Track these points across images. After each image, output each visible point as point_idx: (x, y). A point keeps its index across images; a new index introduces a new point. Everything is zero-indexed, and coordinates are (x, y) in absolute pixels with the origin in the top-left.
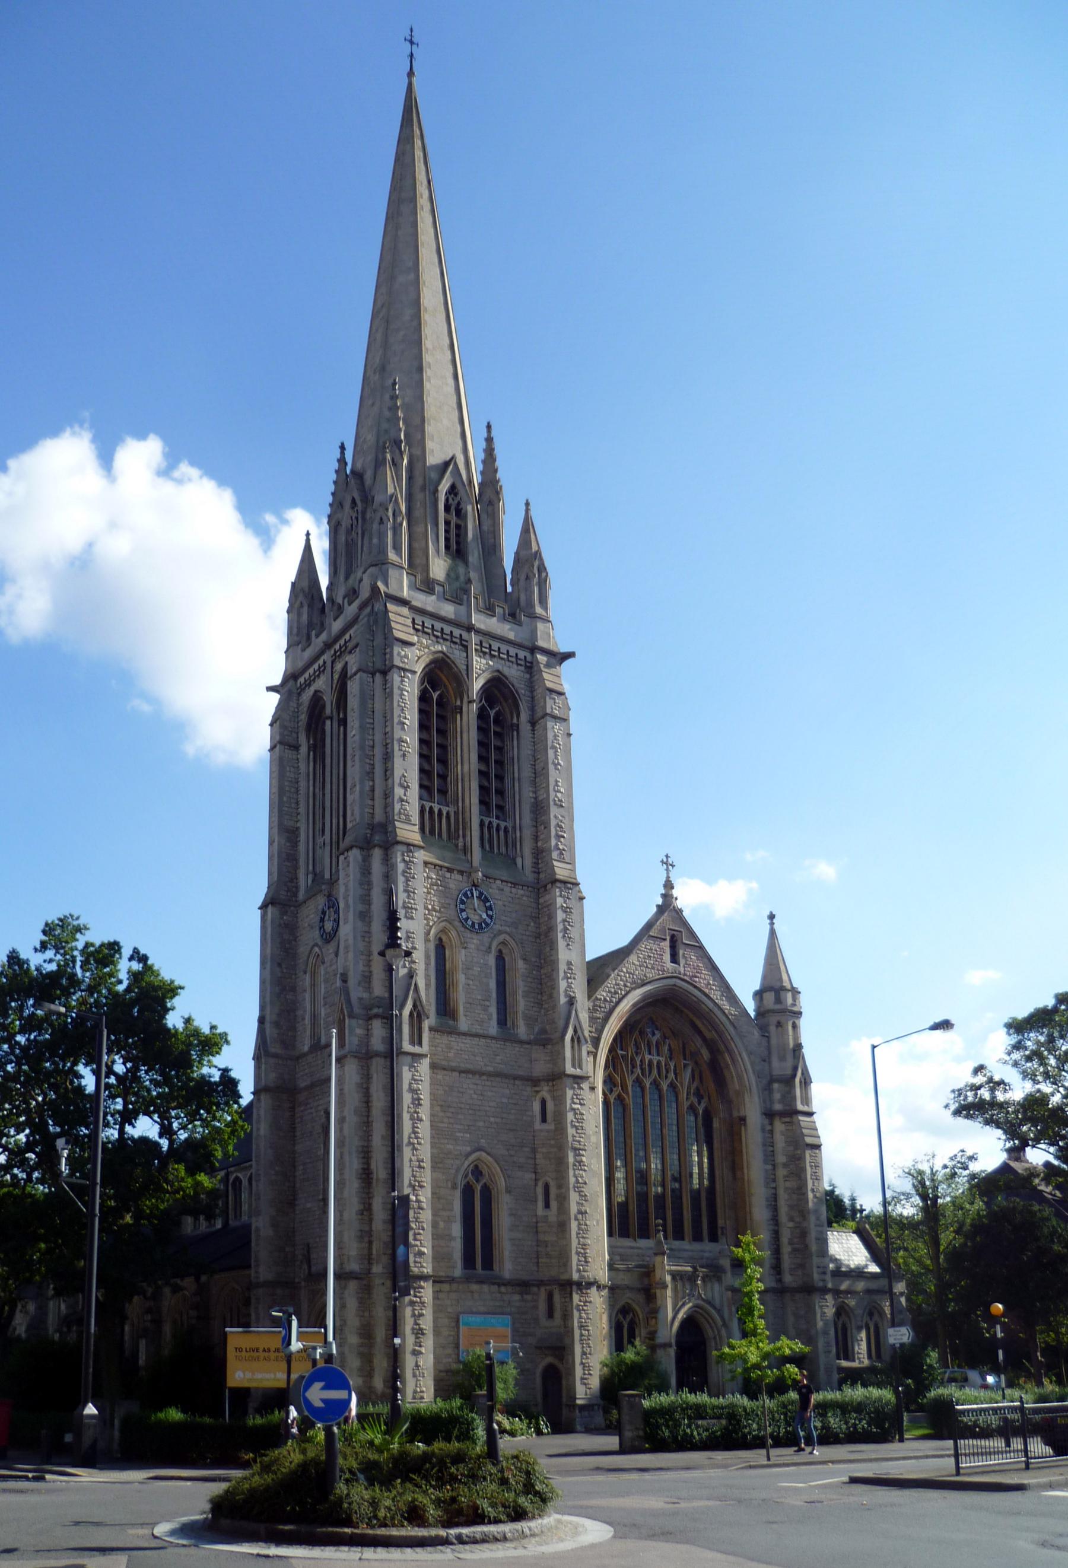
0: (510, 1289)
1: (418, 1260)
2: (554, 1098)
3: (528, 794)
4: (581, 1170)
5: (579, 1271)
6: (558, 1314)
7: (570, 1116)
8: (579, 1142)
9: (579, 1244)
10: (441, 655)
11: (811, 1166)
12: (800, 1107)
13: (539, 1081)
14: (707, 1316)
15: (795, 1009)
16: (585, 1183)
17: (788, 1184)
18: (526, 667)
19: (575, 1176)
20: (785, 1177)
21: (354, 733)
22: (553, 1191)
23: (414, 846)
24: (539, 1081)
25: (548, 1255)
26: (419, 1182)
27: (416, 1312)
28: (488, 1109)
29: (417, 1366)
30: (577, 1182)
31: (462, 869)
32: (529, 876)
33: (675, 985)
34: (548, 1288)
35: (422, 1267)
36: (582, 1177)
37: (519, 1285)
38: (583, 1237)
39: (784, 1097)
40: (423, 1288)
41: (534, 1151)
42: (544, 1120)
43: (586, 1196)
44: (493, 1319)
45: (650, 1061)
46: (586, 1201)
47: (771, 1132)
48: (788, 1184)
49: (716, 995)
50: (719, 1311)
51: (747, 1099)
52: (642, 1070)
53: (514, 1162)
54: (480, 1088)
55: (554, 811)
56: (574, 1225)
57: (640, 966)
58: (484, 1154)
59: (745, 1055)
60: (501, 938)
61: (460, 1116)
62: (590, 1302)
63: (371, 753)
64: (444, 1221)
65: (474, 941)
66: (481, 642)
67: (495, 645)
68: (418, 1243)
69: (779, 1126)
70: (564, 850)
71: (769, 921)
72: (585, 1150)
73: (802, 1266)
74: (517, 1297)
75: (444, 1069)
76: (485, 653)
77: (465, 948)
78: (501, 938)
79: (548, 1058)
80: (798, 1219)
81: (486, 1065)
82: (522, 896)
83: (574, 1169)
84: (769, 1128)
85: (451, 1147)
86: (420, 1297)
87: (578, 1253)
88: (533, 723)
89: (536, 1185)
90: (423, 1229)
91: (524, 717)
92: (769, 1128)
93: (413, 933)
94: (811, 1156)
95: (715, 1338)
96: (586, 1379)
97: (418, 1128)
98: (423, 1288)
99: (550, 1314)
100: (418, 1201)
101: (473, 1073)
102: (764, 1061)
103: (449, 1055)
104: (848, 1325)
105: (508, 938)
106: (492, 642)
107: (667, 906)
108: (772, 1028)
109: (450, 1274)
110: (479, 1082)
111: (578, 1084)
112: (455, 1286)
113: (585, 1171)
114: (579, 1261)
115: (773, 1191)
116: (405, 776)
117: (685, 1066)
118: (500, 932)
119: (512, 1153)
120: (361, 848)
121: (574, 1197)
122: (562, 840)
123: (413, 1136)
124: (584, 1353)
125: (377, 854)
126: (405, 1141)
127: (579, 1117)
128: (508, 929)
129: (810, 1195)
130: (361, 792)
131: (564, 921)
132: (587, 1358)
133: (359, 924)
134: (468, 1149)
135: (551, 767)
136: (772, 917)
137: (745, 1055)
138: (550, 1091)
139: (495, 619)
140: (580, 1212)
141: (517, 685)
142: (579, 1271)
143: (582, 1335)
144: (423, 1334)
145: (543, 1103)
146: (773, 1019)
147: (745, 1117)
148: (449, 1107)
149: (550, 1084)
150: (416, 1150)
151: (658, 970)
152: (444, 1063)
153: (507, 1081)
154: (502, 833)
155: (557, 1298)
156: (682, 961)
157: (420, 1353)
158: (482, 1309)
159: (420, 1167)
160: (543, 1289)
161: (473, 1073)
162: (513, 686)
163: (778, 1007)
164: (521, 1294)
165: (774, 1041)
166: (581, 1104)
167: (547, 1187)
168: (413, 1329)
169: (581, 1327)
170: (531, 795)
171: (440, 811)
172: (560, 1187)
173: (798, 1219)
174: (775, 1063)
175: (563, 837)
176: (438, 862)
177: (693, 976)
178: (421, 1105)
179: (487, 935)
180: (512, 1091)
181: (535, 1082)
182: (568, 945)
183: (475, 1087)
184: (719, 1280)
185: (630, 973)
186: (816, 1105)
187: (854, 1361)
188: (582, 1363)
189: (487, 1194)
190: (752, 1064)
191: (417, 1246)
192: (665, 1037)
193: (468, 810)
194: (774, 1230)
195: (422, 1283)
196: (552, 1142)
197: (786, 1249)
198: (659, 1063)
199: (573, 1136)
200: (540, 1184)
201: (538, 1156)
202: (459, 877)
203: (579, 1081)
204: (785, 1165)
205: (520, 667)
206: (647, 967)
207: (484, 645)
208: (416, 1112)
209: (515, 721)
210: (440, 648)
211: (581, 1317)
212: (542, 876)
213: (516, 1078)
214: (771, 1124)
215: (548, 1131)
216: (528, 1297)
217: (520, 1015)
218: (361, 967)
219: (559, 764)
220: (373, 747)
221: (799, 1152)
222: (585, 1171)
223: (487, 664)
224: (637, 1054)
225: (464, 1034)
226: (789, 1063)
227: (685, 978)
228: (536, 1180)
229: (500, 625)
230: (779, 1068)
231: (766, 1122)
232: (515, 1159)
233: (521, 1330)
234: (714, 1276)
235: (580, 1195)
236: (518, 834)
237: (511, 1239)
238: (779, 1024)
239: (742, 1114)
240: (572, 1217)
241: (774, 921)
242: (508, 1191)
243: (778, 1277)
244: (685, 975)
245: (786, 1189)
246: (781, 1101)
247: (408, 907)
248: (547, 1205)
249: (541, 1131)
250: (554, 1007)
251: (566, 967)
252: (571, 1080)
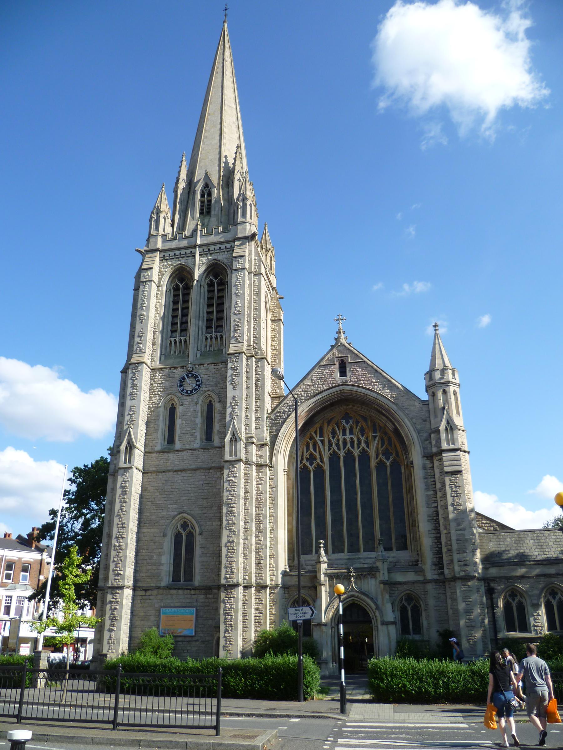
0: (197, 592)
1: (117, 578)
4: (232, 516)
5: (226, 578)
7: (226, 485)
8: (231, 499)
9: (227, 561)
10: (180, 265)
11: (451, 488)
12: (445, 446)
15: (443, 381)
16: (234, 524)
19: (227, 520)
23: (138, 363)
26: (121, 535)
27: (113, 607)
28: (190, 489)
29: (111, 638)
30: (228, 523)
31: (182, 365)
33: (343, 390)
35: (119, 582)
36: (232, 520)
37: (204, 589)
38: (230, 557)
40: (118, 593)
43: (234, 531)
44: (183, 610)
45: (344, 439)
46: (234, 534)
47: (433, 468)
49: (378, 388)
50: (372, 599)
51: (413, 449)
52: (338, 445)
53: (206, 517)
54: (186, 478)
55: (233, 318)
56: (224, 551)
57: (313, 385)
58: (185, 515)
59: (406, 420)
60: (207, 394)
61: (171, 496)
62: (234, 597)
64: (157, 555)
65: (189, 399)
66: (203, 250)
67: (212, 248)
68: (118, 569)
70: (239, 336)
72: (236, 504)
74: (202, 596)
75: (164, 472)
76: (206, 254)
77: (182, 405)
78: (207, 394)
81: (191, 465)
82: (221, 368)
83: (226, 516)
84: (431, 465)
85: (164, 513)
86: (116, 599)
87: (226, 567)
90: (121, 561)
92: (431, 465)
93: (134, 406)
94: (450, 480)
95: (373, 618)
96: (227, 647)
97: (123, 506)
98: (118, 593)
100: (120, 546)
101: (182, 471)
102: (425, 421)
103: (168, 464)
104: (525, 604)
105: (210, 393)
106: (209, 247)
107: (337, 344)
109: (158, 585)
110: (185, 475)
111: (233, 465)
112: (160, 592)
113: (235, 516)
114: (227, 572)
115: (434, 509)
116: (141, 331)
117: (375, 437)
118: (205, 392)
119: (204, 511)
121: (225, 533)
122: (238, 331)
123: (120, 511)
124: (226, 630)
126: (116, 514)
127: (233, 485)
128: (210, 389)
129: (451, 509)
131: (232, 375)
132: (230, 633)
134: (176, 513)
135: (233, 296)
137: (406, 420)
139: (213, 235)
140: (229, 542)
142: (226, 578)
143: (226, 619)
144: (116, 619)
147: (413, 462)
148: (164, 492)
150: (121, 518)
151: (328, 384)
152: (163, 469)
153: (204, 471)
154: (219, 339)
156: (349, 374)
157: (113, 630)
158: (177, 604)
159: (123, 527)
161: (182, 471)
162: (223, 263)
164: (206, 594)
166: (234, 477)
168: (110, 617)
169: (225, 614)
171: (181, 340)
175: (239, 330)
176: (167, 366)
177: (358, 381)
178: (127, 494)
179: (196, 395)
180: (207, 477)
182: (234, 387)
183: (182, 478)
184: (374, 576)
185: (304, 391)
187: (531, 633)
188: (225, 637)
189: (191, 537)
190: (414, 425)
191: (117, 570)
192: (357, 422)
194: (436, 537)
195: (117, 591)
198: (352, 439)
199: (227, 496)
202: (182, 370)
203: (233, 463)
204: (441, 490)
205: (229, 252)
206: (319, 384)
207: (205, 250)
208: (124, 498)
209: (227, 280)
210: (179, 263)
211: (225, 607)
213: (210, 468)
214: (433, 463)
216: (211, 596)
217: (216, 433)
219: (239, 293)
222: (235, 516)
223: (208, 259)
224: (333, 437)
225: (178, 451)
227: (352, 383)
229: (216, 237)
231: (427, 462)
232: (206, 515)
233: (205, 616)
234: (369, 574)
235: (230, 531)
239: (411, 460)
240: (223, 545)
241: (437, 328)
242: (200, 534)
243: (440, 571)
244: (351, 381)
247: (132, 394)
251: (231, 401)
252: (228, 464)
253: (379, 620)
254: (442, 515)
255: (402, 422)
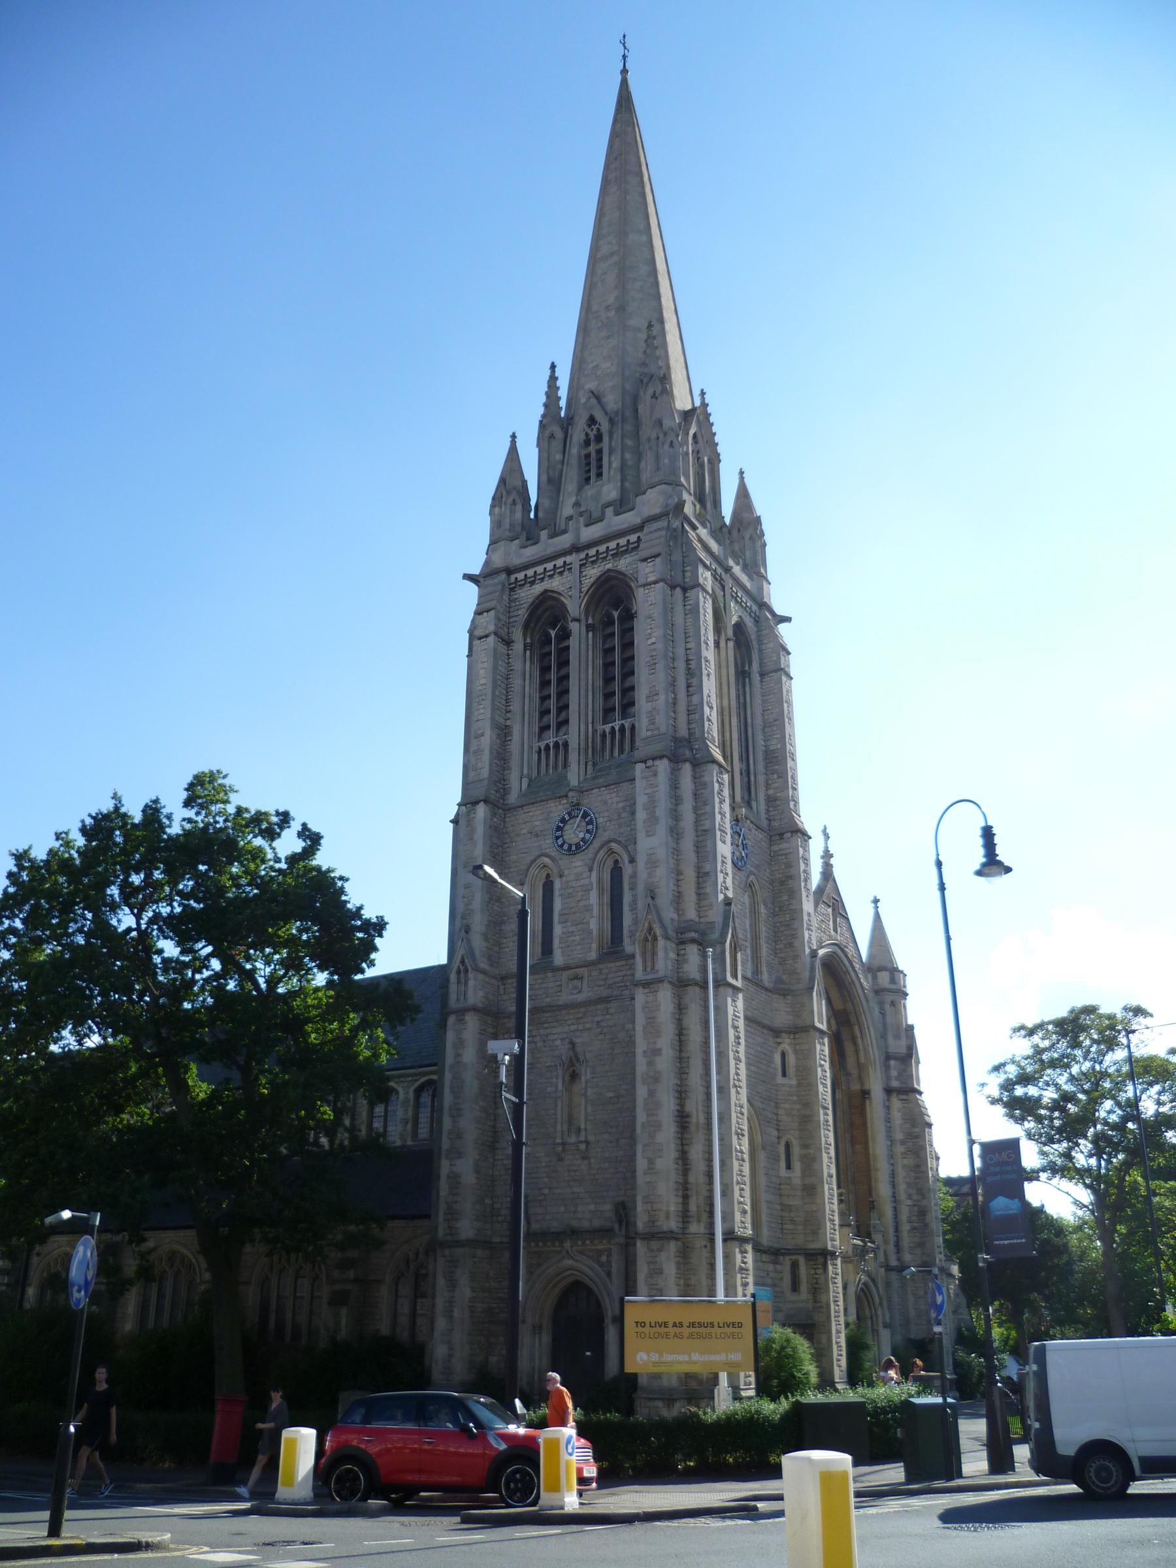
2: (796, 1052)
3: (760, 742)
6: (804, 1287)
13: (781, 1032)
14: (868, 1294)
17: (906, 1162)
18: (755, 620)
20: (903, 1154)
21: (653, 640)
22: (796, 1151)
24: (781, 1032)
25: (792, 1221)
32: (765, 823)
34: (793, 1257)
39: (900, 1075)
41: (777, 1106)
42: (784, 1074)
47: (888, 1108)
48: (906, 1162)
63: (672, 665)
69: (896, 1103)
71: (873, 905)
73: (921, 1245)
79: (789, 1009)
80: (915, 1197)
88: (762, 675)
89: (779, 1143)
91: (755, 666)
95: (871, 1318)
99: (795, 1287)
108: (887, 1007)
120: (670, 760)
125: (687, 767)
130: (667, 701)
133: (670, 839)
136: (876, 901)
138: (790, 1044)
141: (750, 633)
145: (783, 1055)
146: (888, 998)
149: (792, 1036)
155: (803, 1270)
160: (787, 1258)
163: (893, 987)
165: (889, 1019)
167: (788, 1146)
170: (763, 743)
172: (805, 1146)
173: (915, 1197)
174: (891, 1040)
181: (776, 1032)
186: (922, 1087)
193: (728, 743)
196: (795, 1098)
197: (905, 1227)
200: (783, 1143)
201: (781, 1112)
204: (903, 1143)
209: (747, 668)
212: (775, 824)
215: (791, 1086)
217: (763, 960)
218: (672, 887)
220: (674, 659)
221: (917, 1130)
226: (903, 1042)
228: (779, 1138)
230: (897, 1046)
236: (752, 778)
237: (768, 1202)
238: (893, 1004)
239: (867, 1087)
241: (879, 904)
245: (904, 1166)
246: (897, 1079)
248: (789, 1167)
249: (783, 1085)
250: (796, 957)
252: (817, 1034)
253: (880, 1319)
254: (904, 1178)
255: (867, 1030)
